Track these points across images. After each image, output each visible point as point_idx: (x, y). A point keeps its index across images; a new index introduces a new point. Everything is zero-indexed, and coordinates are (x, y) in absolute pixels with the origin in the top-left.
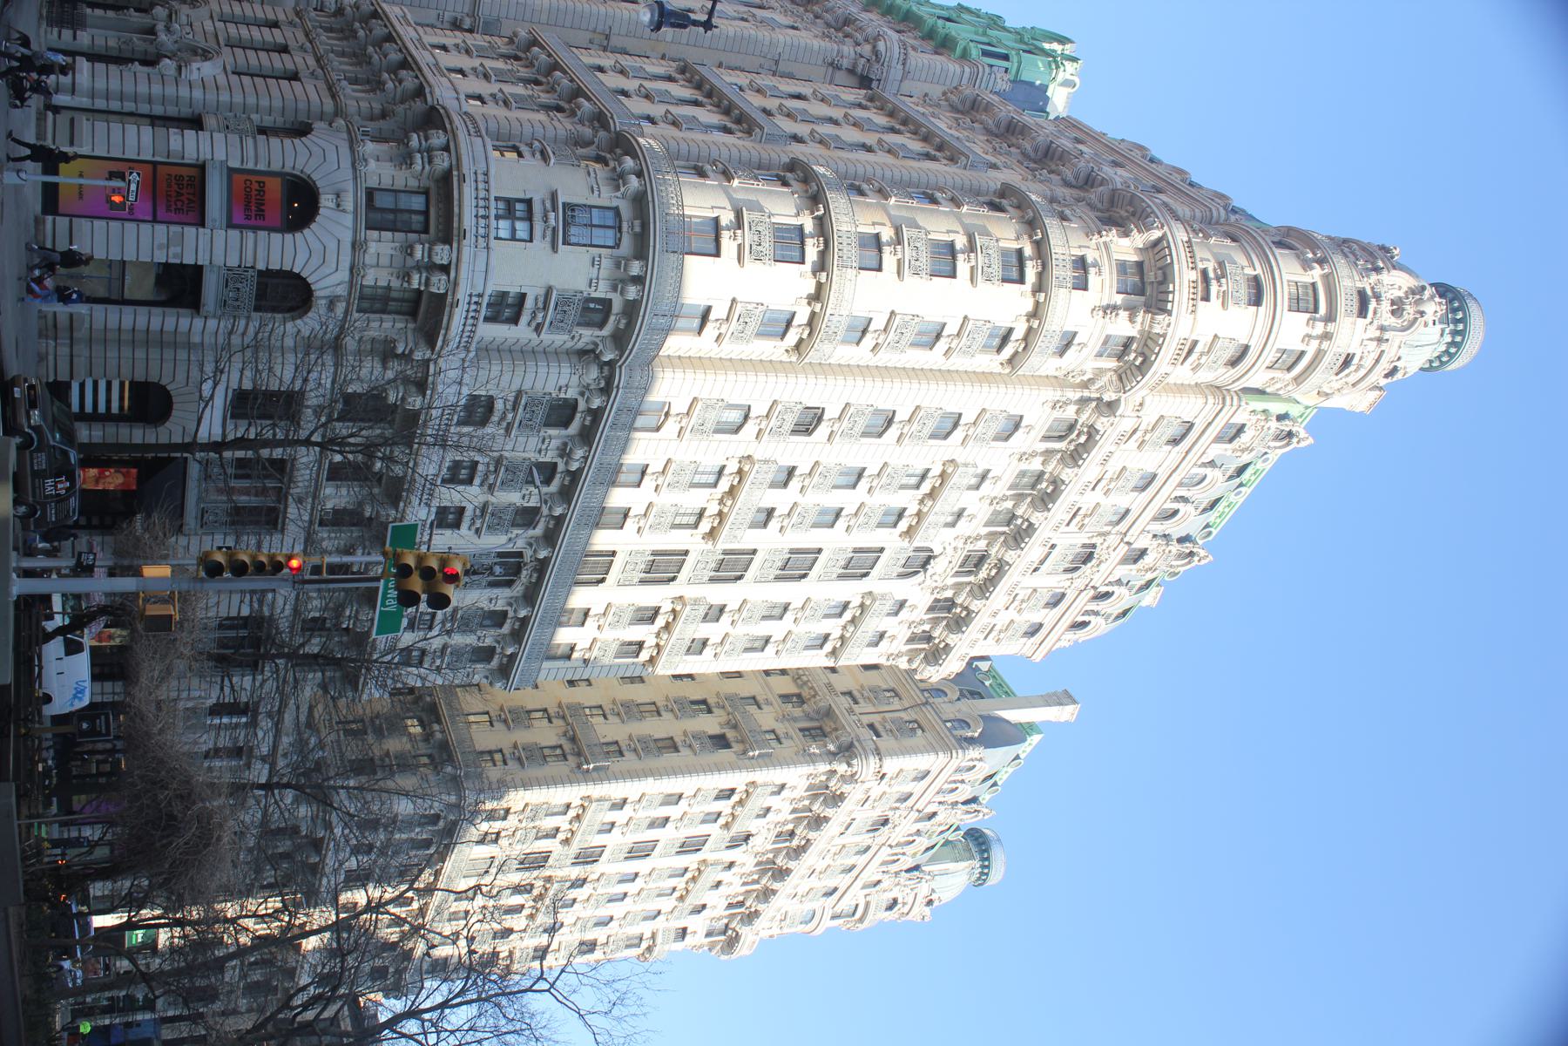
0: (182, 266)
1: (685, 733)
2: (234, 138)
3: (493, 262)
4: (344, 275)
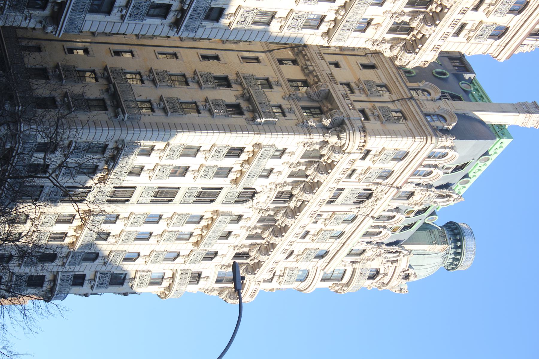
1: (206, 100)
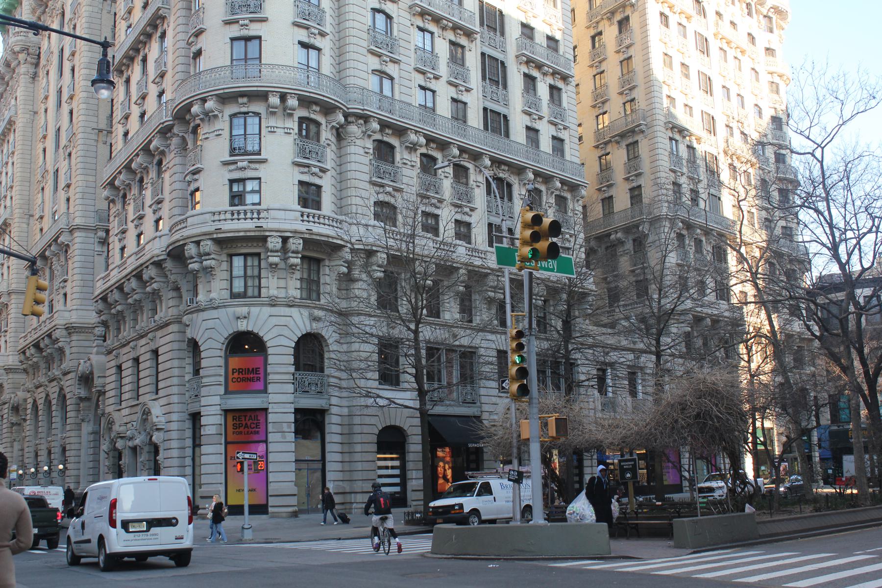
0: (296, 421)
1: (618, 52)
2: (204, 391)
3: (277, 206)
4: (294, 311)
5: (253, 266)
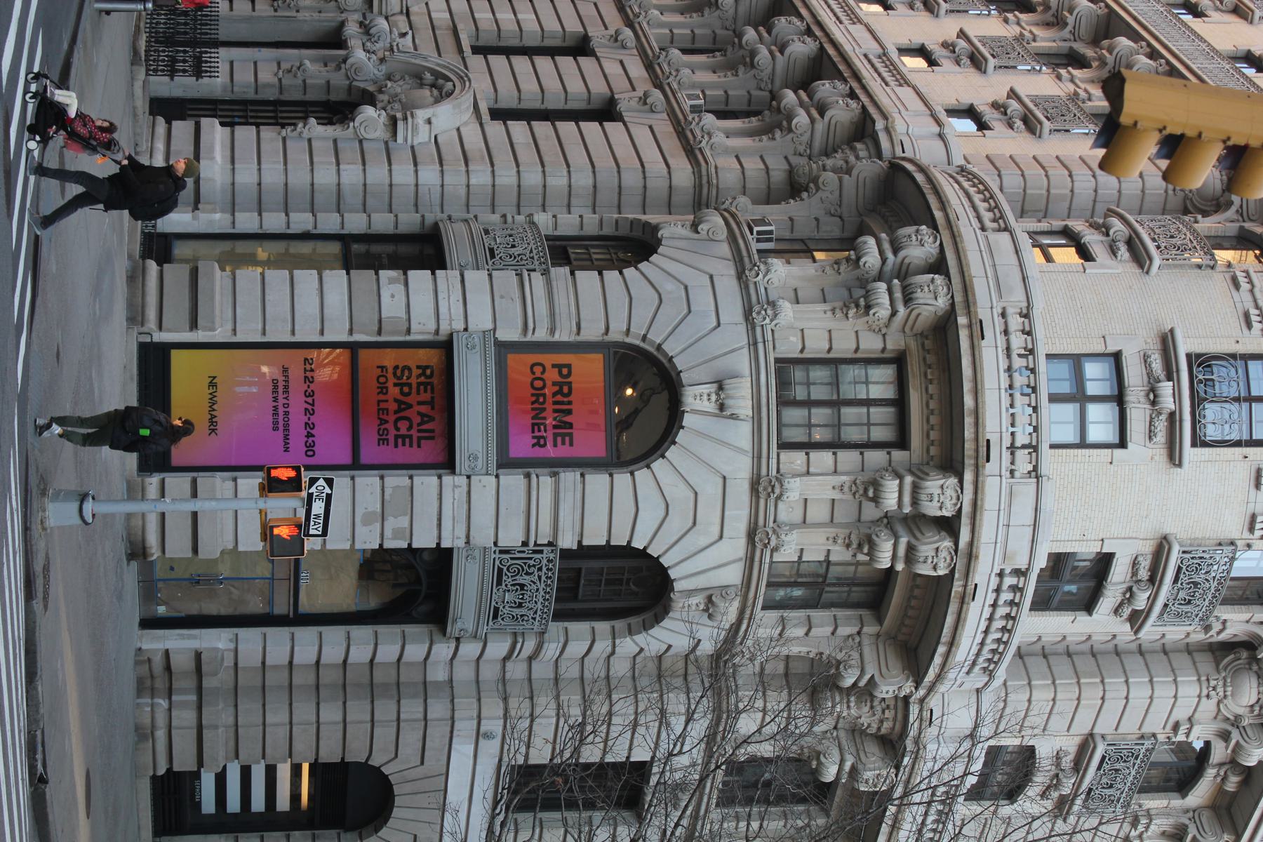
2: (507, 279)
3: (1047, 502)
4: (735, 546)
5: (869, 424)
